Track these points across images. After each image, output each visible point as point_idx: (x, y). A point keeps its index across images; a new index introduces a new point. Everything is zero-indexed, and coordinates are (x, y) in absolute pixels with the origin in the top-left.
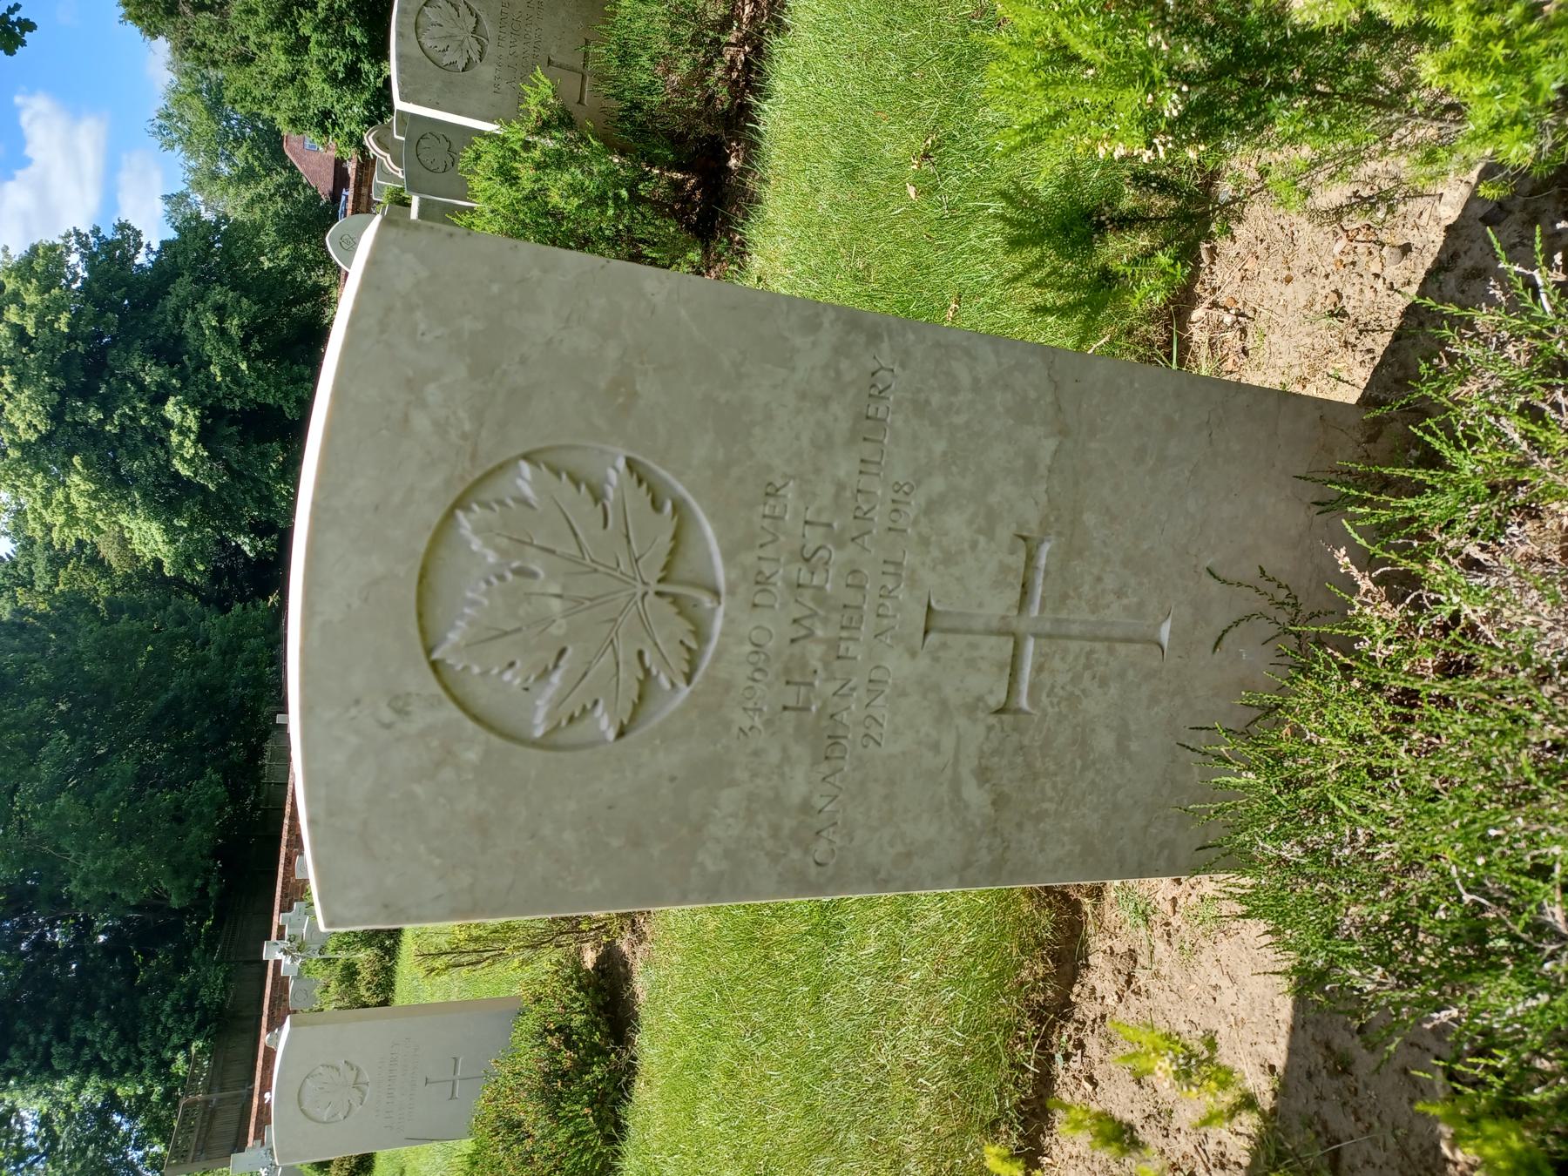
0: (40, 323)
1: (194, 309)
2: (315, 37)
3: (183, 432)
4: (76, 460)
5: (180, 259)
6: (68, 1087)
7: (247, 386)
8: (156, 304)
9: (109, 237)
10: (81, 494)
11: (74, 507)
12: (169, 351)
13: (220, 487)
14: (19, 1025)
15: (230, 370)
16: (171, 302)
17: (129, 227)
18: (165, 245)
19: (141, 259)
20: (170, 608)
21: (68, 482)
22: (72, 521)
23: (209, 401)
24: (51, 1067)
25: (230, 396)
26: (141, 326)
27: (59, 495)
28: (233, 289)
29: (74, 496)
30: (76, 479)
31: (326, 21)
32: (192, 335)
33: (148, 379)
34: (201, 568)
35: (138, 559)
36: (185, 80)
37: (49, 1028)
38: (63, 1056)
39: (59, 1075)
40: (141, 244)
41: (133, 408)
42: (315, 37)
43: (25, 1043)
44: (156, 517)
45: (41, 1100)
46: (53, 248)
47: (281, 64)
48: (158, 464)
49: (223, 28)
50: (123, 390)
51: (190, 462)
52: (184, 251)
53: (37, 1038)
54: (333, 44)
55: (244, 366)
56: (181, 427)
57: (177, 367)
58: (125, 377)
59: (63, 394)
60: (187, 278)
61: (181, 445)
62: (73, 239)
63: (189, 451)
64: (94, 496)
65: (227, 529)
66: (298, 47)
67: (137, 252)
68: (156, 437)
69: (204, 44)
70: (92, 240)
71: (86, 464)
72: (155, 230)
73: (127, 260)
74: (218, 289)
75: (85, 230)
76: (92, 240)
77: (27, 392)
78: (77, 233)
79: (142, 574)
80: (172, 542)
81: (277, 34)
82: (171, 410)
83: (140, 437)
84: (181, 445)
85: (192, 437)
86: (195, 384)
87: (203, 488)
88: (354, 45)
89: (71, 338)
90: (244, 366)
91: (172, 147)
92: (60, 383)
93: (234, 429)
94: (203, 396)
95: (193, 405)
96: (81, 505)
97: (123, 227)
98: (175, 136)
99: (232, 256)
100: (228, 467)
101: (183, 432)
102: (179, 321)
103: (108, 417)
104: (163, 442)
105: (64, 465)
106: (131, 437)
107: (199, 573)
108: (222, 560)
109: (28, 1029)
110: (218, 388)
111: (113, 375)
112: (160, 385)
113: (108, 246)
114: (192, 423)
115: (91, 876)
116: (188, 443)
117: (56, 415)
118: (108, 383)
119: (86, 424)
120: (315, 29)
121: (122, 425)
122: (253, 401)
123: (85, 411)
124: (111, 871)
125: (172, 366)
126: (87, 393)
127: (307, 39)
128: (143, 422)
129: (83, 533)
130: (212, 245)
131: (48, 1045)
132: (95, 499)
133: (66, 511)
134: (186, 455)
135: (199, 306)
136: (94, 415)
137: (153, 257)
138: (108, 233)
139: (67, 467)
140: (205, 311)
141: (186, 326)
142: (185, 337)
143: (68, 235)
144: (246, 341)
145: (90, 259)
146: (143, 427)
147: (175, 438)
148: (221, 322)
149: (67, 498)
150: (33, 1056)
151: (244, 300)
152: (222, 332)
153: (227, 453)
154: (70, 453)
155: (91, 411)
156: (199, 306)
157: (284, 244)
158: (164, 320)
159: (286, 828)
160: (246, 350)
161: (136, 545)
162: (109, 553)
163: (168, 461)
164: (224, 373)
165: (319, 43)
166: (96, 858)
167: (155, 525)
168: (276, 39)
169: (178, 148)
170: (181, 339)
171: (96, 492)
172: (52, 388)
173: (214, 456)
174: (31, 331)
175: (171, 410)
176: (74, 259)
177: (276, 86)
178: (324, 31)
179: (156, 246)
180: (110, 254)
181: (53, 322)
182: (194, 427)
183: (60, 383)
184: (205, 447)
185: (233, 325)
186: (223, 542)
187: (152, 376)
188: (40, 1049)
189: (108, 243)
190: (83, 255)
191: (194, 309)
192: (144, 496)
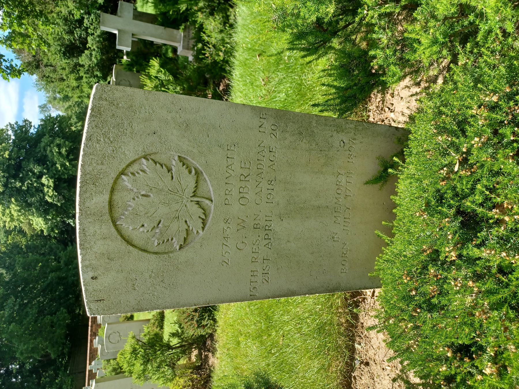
1: (50, 146)
2: (84, 76)
3: (48, 187)
4: (13, 200)
5: (45, 130)
7: (69, 170)
8: (37, 145)
9: (21, 125)
10: (15, 211)
11: (13, 215)
12: (42, 161)
13: (62, 204)
15: (63, 165)
16: (42, 144)
17: (28, 121)
18: (39, 126)
19: (32, 131)
20: (47, 246)
21: (10, 207)
22: (12, 220)
23: (57, 176)
25: (63, 174)
26: (33, 153)
27: (7, 211)
28: (63, 139)
29: (13, 212)
30: (13, 206)
31: (88, 70)
32: (50, 155)
33: (36, 171)
34: (57, 232)
35: (34, 230)
40: (31, 126)
41: (31, 181)
42: (84, 76)
44: (41, 216)
47: (75, 84)
48: (40, 197)
49: (55, 71)
50: (28, 175)
51: (51, 197)
52: (46, 127)
54: (91, 77)
55: (68, 164)
56: (47, 186)
57: (45, 166)
58: (28, 171)
59: (8, 178)
60: (47, 136)
61: (48, 192)
62: (9, 127)
63: (51, 193)
64: (19, 211)
65: (65, 217)
66: (80, 78)
67: (30, 128)
68: (40, 190)
69: (49, 76)
70: (15, 126)
71: (16, 200)
72: (36, 121)
73: (27, 131)
74: (58, 139)
75: (13, 122)
76: (15, 126)
78: (10, 124)
79: (37, 235)
80: (46, 224)
81: (72, 75)
82: (44, 180)
83: (34, 190)
84: (48, 192)
85: (52, 188)
86: (52, 171)
87: (56, 205)
88: (97, 76)
89: (9, 159)
90: (68, 164)
91: (41, 90)
92: (6, 175)
93: (65, 185)
94: (55, 174)
95: (51, 178)
96: (15, 214)
97: (25, 121)
98: (42, 87)
99: (62, 128)
100: (64, 197)
101: (48, 187)
102: (45, 150)
103: (23, 184)
104: (42, 191)
105: (9, 202)
106: (31, 190)
107: (56, 233)
108: (64, 227)
110: (59, 171)
111: (24, 170)
112: (40, 172)
113: (21, 128)
114: (51, 184)
115: (23, 351)
116: (50, 191)
117: (5, 185)
118: (22, 173)
119: (16, 187)
120: (85, 73)
121: (28, 187)
122: (72, 175)
123: (15, 183)
124: (30, 349)
125: (44, 165)
126: (15, 177)
127: (82, 77)
128: (35, 185)
129: (16, 223)
130: (55, 124)
132: (20, 212)
133: (10, 217)
134: (50, 195)
135: (52, 145)
136: (18, 184)
137: (36, 130)
138: (21, 123)
139: (10, 202)
140: (54, 147)
141: (48, 152)
142: (47, 156)
143: (7, 125)
144: (68, 156)
145: (15, 132)
146: (35, 187)
147: (46, 189)
148: (59, 150)
149: (10, 212)
151: (67, 143)
152: (60, 153)
153: (64, 193)
154: (10, 198)
155: (17, 183)
156: (52, 145)
157: (80, 121)
158: (40, 151)
159: (89, 330)
160: (68, 158)
161: (35, 226)
162: (26, 228)
163: (44, 197)
164: (61, 166)
165: (86, 77)
166: (24, 344)
167: (40, 219)
168: (72, 76)
169: (43, 90)
170: (46, 156)
171: (20, 210)
172: (4, 177)
173: (59, 194)
175: (44, 180)
176: (10, 132)
177: (73, 89)
178: (88, 73)
179: (37, 126)
180: (22, 130)
181: (3, 155)
182: (52, 185)
183: (6, 175)
184: (56, 192)
185: (63, 151)
186: (64, 222)
187: (37, 169)
189: (21, 126)
190: (13, 131)
191: (50, 146)
192: (36, 209)
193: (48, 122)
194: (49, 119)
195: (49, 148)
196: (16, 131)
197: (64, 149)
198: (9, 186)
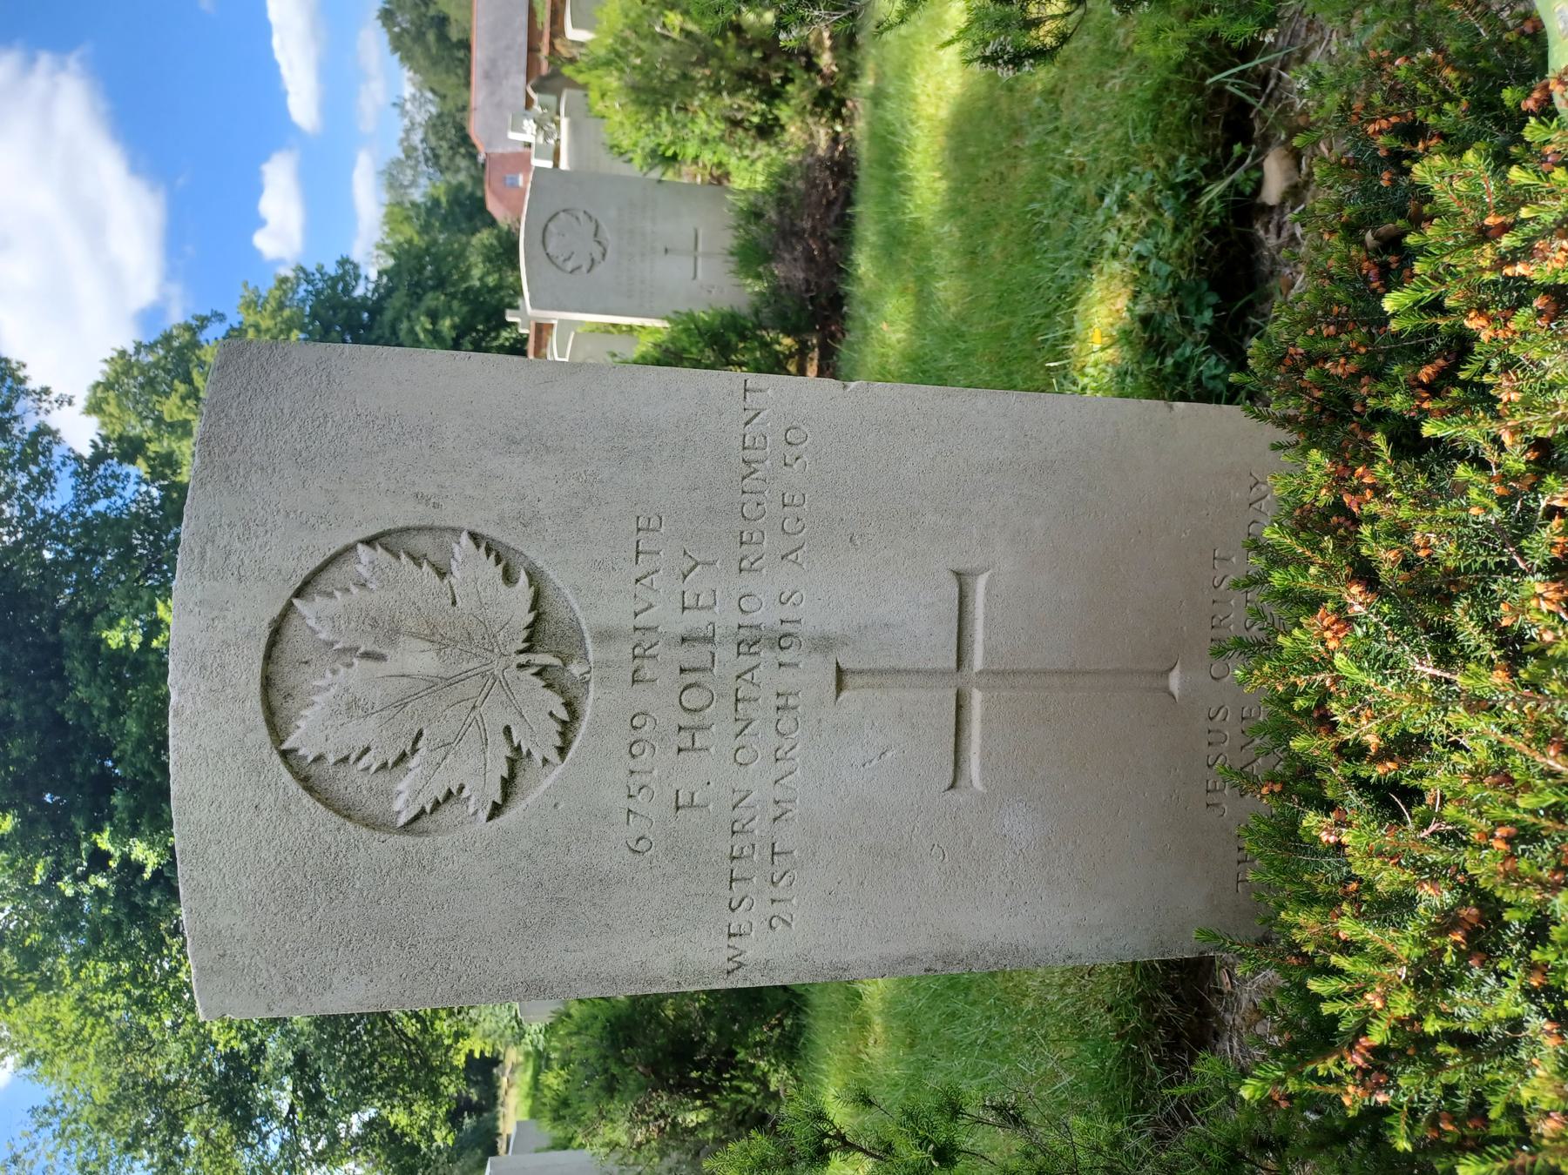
1: (409, 317)
9: (333, 274)
16: (388, 315)
19: (359, 292)
36: (396, 210)
73: (347, 290)
75: (311, 268)
76: (318, 276)
97: (343, 262)
113: (334, 281)
135: (413, 314)
138: (332, 269)
148: (434, 323)
156: (413, 314)
185: (446, 323)
189: (332, 278)
191: (409, 317)
193: (404, 258)
194: (408, 252)
195: (404, 325)
196: (318, 293)
197: (447, 323)
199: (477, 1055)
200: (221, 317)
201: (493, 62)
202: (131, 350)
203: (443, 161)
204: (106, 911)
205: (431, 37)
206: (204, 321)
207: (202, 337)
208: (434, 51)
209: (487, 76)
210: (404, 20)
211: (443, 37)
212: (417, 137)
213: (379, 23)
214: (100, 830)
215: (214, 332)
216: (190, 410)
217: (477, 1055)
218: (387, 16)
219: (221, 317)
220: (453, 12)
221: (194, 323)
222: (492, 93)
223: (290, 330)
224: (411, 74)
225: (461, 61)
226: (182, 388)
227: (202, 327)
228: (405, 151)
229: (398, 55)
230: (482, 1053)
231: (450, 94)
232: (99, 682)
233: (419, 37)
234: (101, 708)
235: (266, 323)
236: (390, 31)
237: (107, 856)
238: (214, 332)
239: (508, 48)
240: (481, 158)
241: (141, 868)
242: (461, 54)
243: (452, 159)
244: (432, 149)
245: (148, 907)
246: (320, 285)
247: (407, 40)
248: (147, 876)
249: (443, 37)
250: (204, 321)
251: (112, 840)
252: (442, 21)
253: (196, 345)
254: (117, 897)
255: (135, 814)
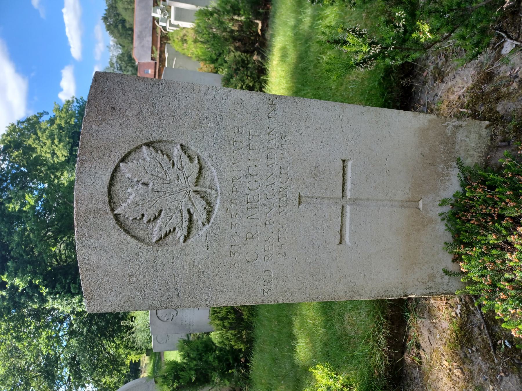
0: (66, 122)
6: (77, 300)
14: (59, 276)
24: (70, 292)
37: (70, 278)
38: (75, 288)
39: (73, 296)
43: (61, 283)
45: (69, 306)
46: (68, 102)
53: (66, 281)
59: (72, 147)
62: (75, 100)
75: (79, 98)
77: (62, 144)
109: (62, 278)
131: (69, 284)
150: (65, 288)
172: (69, 142)
174: (63, 125)
181: (69, 122)
183: (72, 141)
188: (67, 286)
198: (74, 153)
199: (134, 362)
200: (47, 113)
201: (141, 32)
202: (16, 124)
203: (123, 68)
204: (5, 304)
205: (120, 26)
206: (41, 115)
207: (41, 120)
208: (121, 31)
209: (139, 37)
210: (111, 21)
211: (124, 27)
212: (114, 60)
213: (102, 21)
214: (3, 274)
215: (45, 118)
216: (37, 144)
217: (134, 362)
218: (105, 19)
219: (47, 113)
220: (127, 18)
221: (37, 115)
222: (140, 43)
223: (71, 118)
224: (113, 38)
225: (130, 34)
226: (34, 136)
227: (41, 117)
228: (110, 64)
229: (108, 32)
230: (135, 361)
231: (126, 45)
232: (4, 223)
233: (116, 26)
234: (5, 232)
235: (63, 115)
236: (106, 24)
237: (6, 283)
238: (45, 118)
239: (146, 28)
240: (137, 64)
241: (17, 288)
242: (130, 32)
243: (126, 67)
244: (120, 65)
245: (20, 303)
246: (82, 104)
247: (112, 27)
248: (20, 291)
249: (124, 27)
250: (41, 115)
251: (8, 278)
252: (124, 21)
253: (38, 123)
254: (9, 299)
255: (16, 270)
